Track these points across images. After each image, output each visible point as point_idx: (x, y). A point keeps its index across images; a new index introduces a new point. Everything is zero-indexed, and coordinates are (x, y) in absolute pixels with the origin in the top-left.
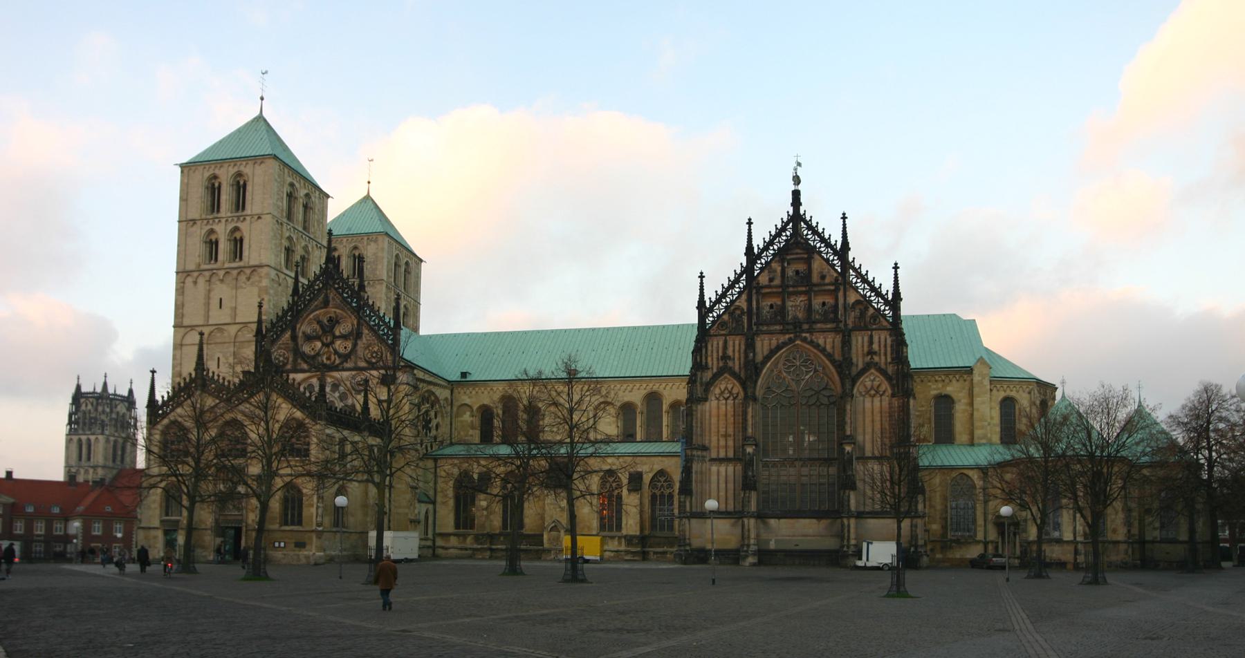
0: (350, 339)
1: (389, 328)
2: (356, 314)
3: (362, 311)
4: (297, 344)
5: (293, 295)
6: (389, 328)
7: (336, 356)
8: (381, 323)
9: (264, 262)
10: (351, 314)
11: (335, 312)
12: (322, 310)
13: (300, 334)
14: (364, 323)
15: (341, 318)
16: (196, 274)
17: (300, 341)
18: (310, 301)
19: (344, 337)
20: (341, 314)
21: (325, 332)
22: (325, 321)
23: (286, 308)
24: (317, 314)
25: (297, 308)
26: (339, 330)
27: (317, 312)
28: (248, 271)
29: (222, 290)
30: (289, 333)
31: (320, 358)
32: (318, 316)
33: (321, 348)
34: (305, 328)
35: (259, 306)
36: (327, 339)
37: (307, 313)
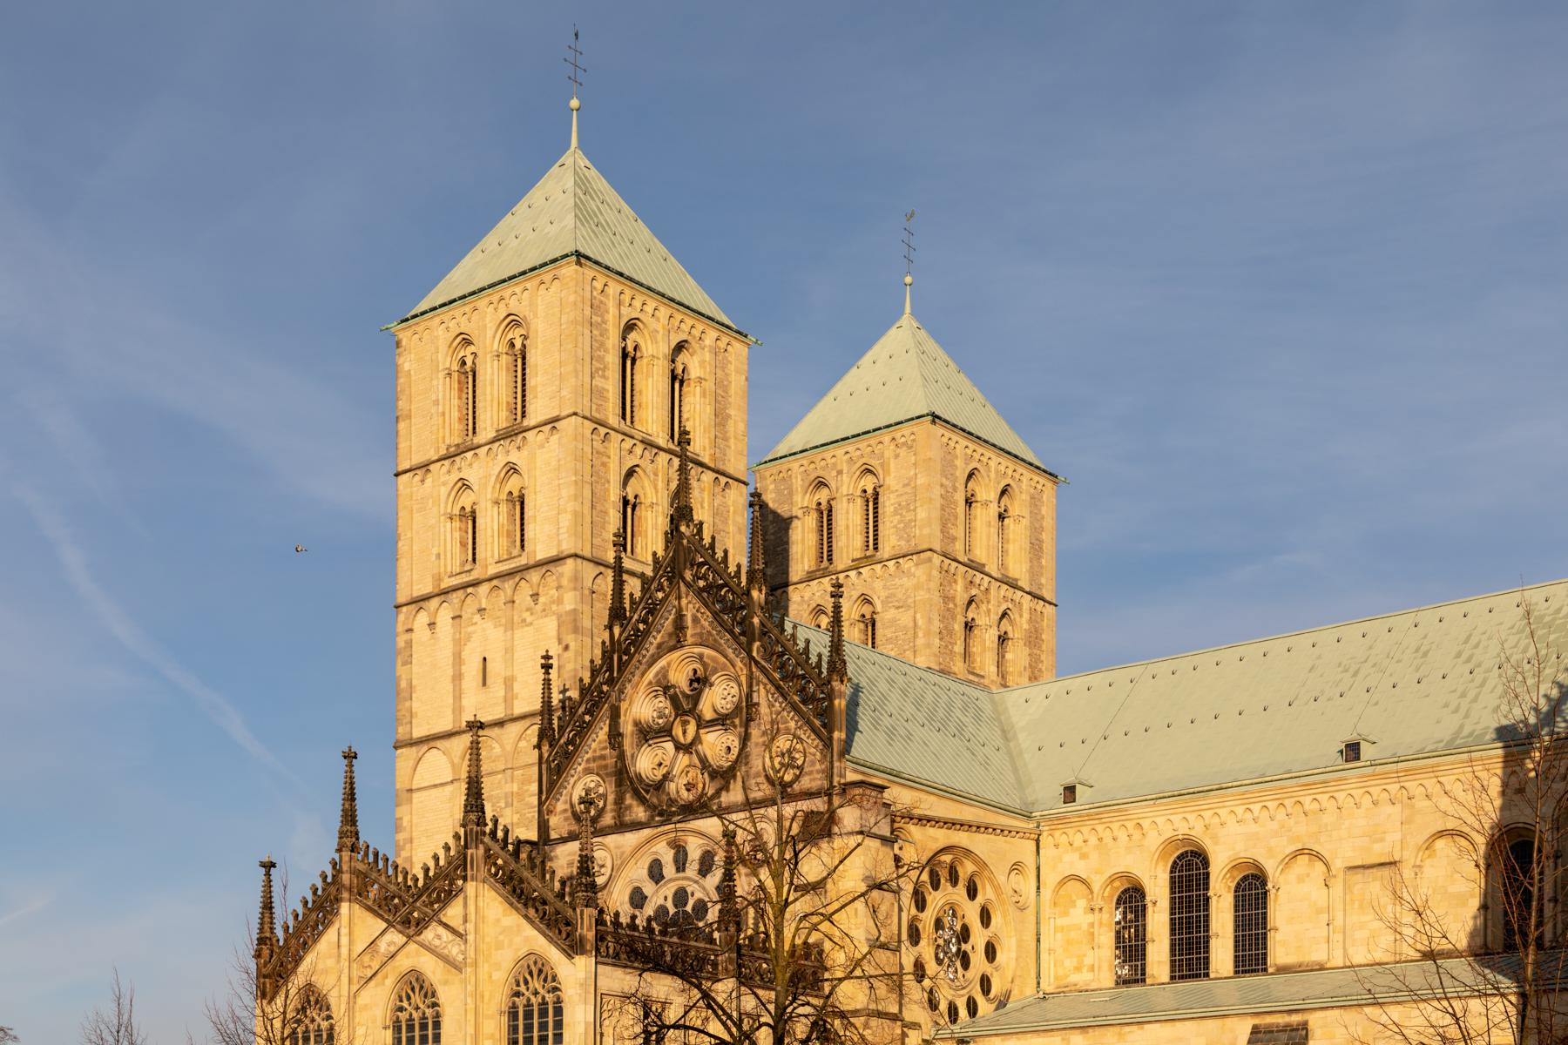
0: (735, 727)
3: (757, 644)
4: (621, 756)
5: (610, 627)
7: (706, 775)
10: (732, 656)
11: (701, 657)
12: (676, 655)
13: (627, 728)
14: (762, 677)
15: (715, 671)
16: (435, 602)
18: (647, 633)
19: (722, 721)
20: (714, 659)
23: (598, 662)
24: (662, 668)
25: (620, 659)
28: (534, 576)
29: (486, 636)
30: (606, 729)
31: (672, 787)
32: (664, 673)
33: (675, 758)
34: (642, 706)
35: (543, 666)
36: (684, 732)
37: (642, 668)
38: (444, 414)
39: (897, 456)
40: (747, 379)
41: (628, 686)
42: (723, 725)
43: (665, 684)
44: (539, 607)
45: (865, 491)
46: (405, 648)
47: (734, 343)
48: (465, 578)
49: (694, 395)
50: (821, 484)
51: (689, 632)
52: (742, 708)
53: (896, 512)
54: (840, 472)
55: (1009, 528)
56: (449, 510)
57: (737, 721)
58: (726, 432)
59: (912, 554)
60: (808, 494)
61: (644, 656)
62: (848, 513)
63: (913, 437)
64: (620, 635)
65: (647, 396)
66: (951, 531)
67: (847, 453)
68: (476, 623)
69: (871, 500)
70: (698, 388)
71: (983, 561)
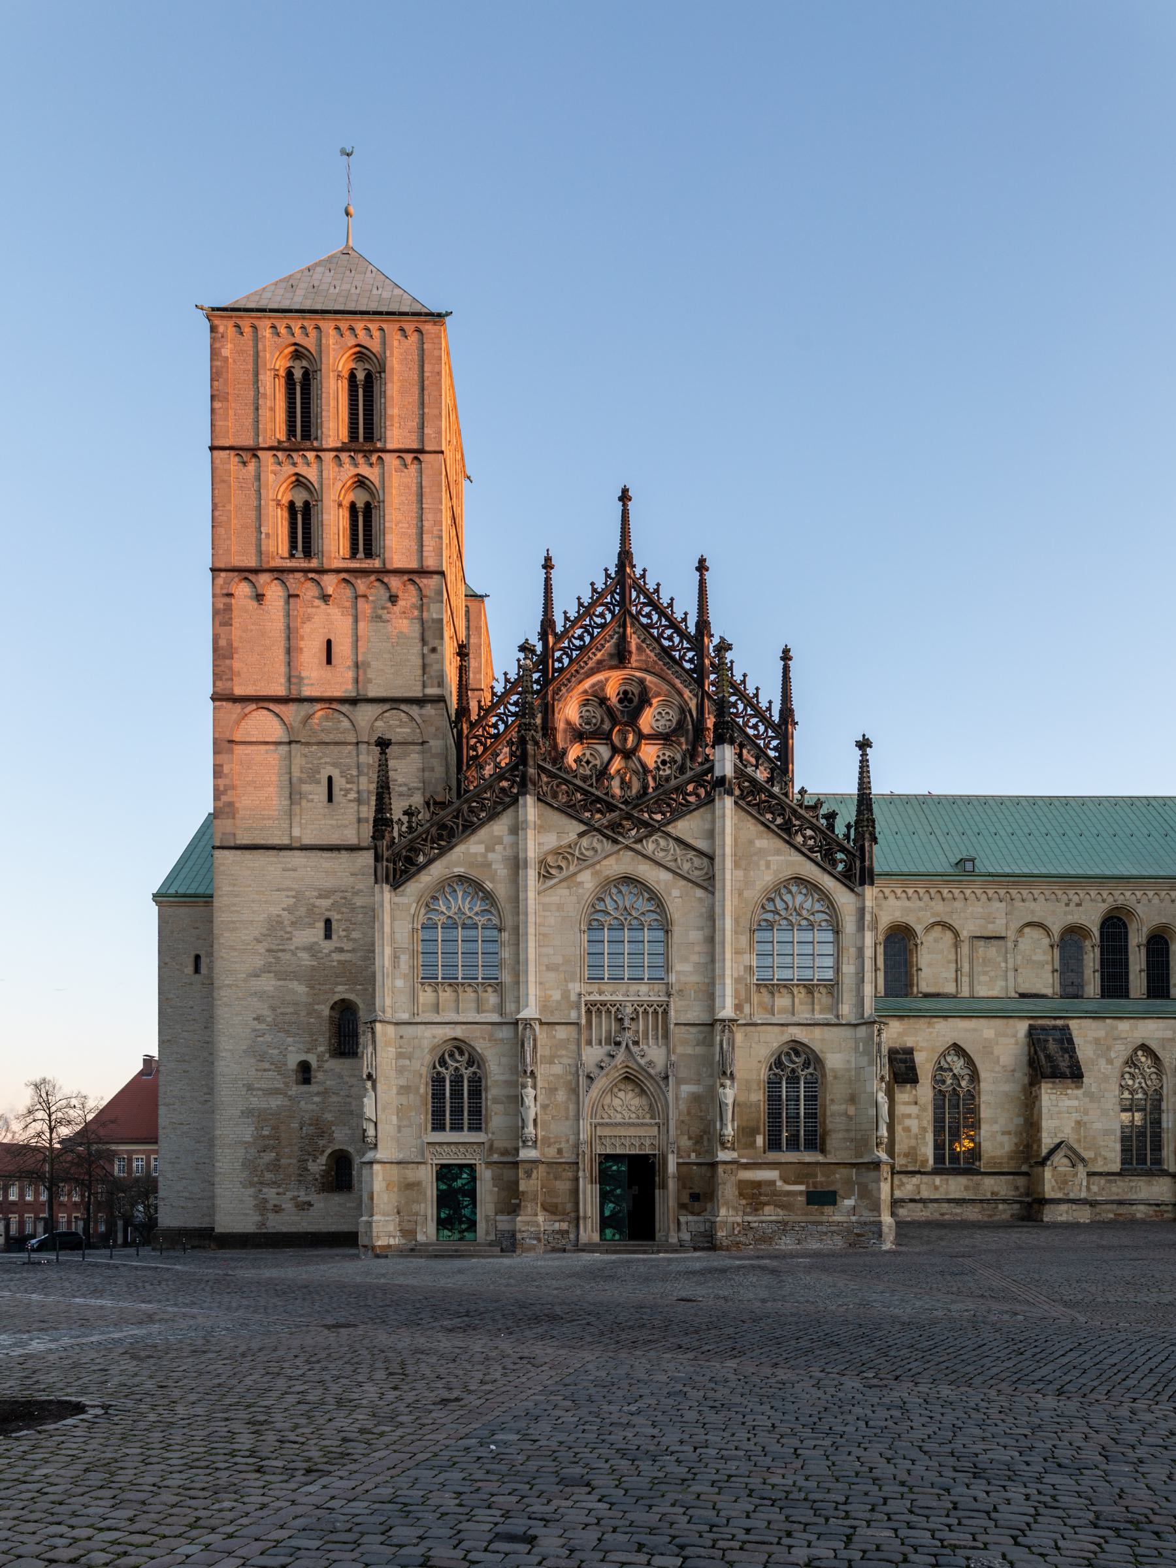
1: (769, 724)
2: (694, 686)
4: (555, 746)
6: (769, 724)
8: (749, 711)
9: (430, 563)
10: (679, 685)
11: (641, 682)
13: (561, 726)
17: (560, 737)
21: (614, 722)
22: (614, 700)
24: (599, 682)
26: (648, 720)
27: (599, 677)
28: (395, 582)
32: (602, 685)
36: (626, 739)
42: (665, 739)
43: (601, 695)
44: (397, 609)
46: (225, 610)
48: (304, 564)
51: (634, 658)
52: (688, 730)
57: (683, 740)
61: (582, 668)
68: (318, 607)
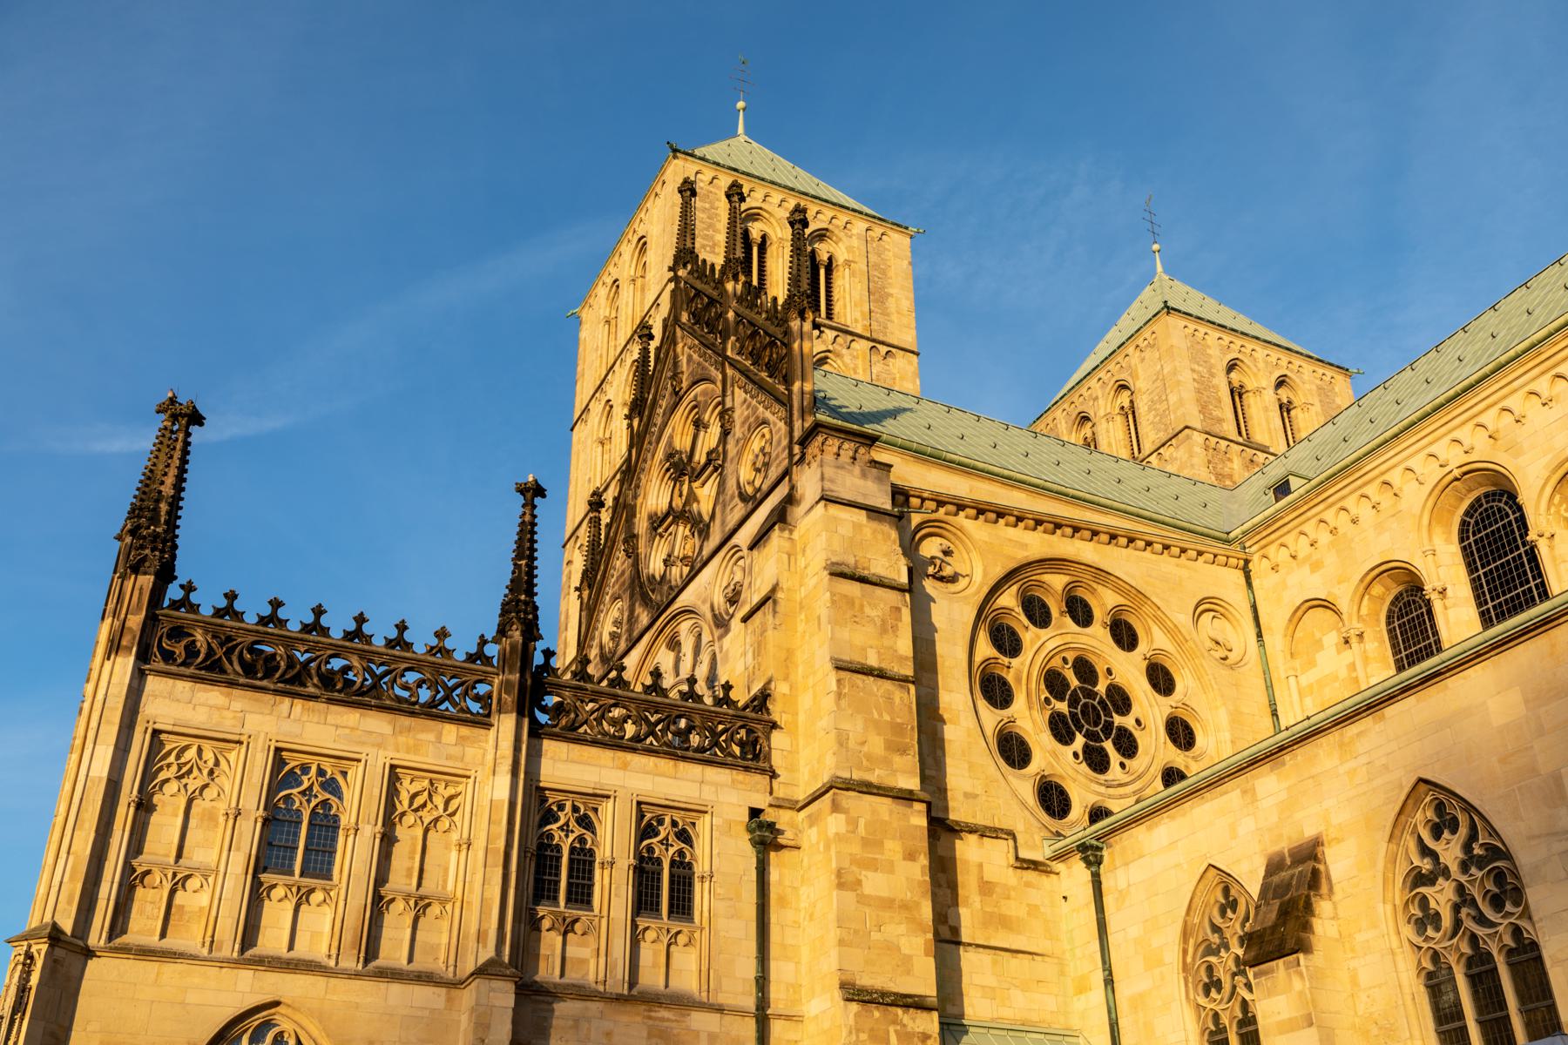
38: (601, 356)
39: (1143, 360)
40: (910, 263)
41: (642, 477)
45: (1122, 408)
47: (889, 232)
49: (844, 278)
50: (1084, 419)
53: (1150, 410)
54: (1096, 399)
55: (1297, 418)
56: (601, 435)
58: (887, 308)
59: (1170, 439)
60: (1074, 433)
62: (1108, 431)
63: (1154, 336)
64: (639, 425)
65: (777, 275)
66: (1214, 413)
67: (1100, 379)
69: (1130, 412)
70: (847, 270)
71: (1267, 444)
